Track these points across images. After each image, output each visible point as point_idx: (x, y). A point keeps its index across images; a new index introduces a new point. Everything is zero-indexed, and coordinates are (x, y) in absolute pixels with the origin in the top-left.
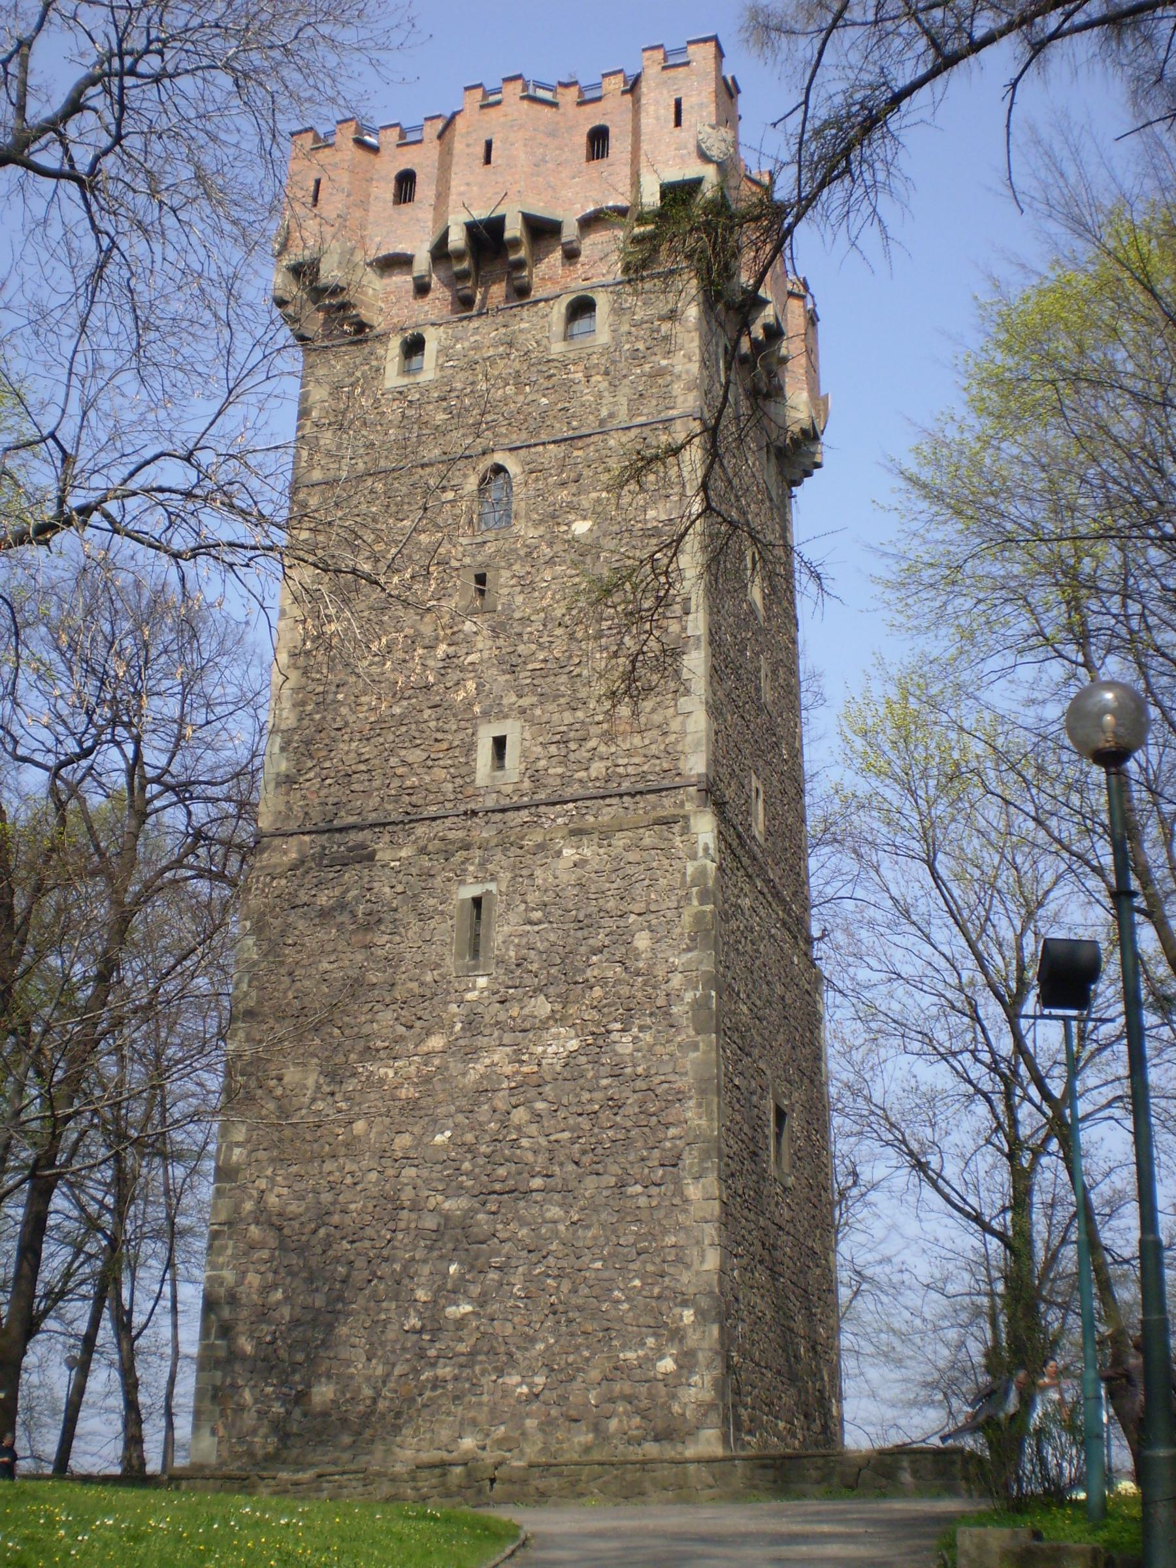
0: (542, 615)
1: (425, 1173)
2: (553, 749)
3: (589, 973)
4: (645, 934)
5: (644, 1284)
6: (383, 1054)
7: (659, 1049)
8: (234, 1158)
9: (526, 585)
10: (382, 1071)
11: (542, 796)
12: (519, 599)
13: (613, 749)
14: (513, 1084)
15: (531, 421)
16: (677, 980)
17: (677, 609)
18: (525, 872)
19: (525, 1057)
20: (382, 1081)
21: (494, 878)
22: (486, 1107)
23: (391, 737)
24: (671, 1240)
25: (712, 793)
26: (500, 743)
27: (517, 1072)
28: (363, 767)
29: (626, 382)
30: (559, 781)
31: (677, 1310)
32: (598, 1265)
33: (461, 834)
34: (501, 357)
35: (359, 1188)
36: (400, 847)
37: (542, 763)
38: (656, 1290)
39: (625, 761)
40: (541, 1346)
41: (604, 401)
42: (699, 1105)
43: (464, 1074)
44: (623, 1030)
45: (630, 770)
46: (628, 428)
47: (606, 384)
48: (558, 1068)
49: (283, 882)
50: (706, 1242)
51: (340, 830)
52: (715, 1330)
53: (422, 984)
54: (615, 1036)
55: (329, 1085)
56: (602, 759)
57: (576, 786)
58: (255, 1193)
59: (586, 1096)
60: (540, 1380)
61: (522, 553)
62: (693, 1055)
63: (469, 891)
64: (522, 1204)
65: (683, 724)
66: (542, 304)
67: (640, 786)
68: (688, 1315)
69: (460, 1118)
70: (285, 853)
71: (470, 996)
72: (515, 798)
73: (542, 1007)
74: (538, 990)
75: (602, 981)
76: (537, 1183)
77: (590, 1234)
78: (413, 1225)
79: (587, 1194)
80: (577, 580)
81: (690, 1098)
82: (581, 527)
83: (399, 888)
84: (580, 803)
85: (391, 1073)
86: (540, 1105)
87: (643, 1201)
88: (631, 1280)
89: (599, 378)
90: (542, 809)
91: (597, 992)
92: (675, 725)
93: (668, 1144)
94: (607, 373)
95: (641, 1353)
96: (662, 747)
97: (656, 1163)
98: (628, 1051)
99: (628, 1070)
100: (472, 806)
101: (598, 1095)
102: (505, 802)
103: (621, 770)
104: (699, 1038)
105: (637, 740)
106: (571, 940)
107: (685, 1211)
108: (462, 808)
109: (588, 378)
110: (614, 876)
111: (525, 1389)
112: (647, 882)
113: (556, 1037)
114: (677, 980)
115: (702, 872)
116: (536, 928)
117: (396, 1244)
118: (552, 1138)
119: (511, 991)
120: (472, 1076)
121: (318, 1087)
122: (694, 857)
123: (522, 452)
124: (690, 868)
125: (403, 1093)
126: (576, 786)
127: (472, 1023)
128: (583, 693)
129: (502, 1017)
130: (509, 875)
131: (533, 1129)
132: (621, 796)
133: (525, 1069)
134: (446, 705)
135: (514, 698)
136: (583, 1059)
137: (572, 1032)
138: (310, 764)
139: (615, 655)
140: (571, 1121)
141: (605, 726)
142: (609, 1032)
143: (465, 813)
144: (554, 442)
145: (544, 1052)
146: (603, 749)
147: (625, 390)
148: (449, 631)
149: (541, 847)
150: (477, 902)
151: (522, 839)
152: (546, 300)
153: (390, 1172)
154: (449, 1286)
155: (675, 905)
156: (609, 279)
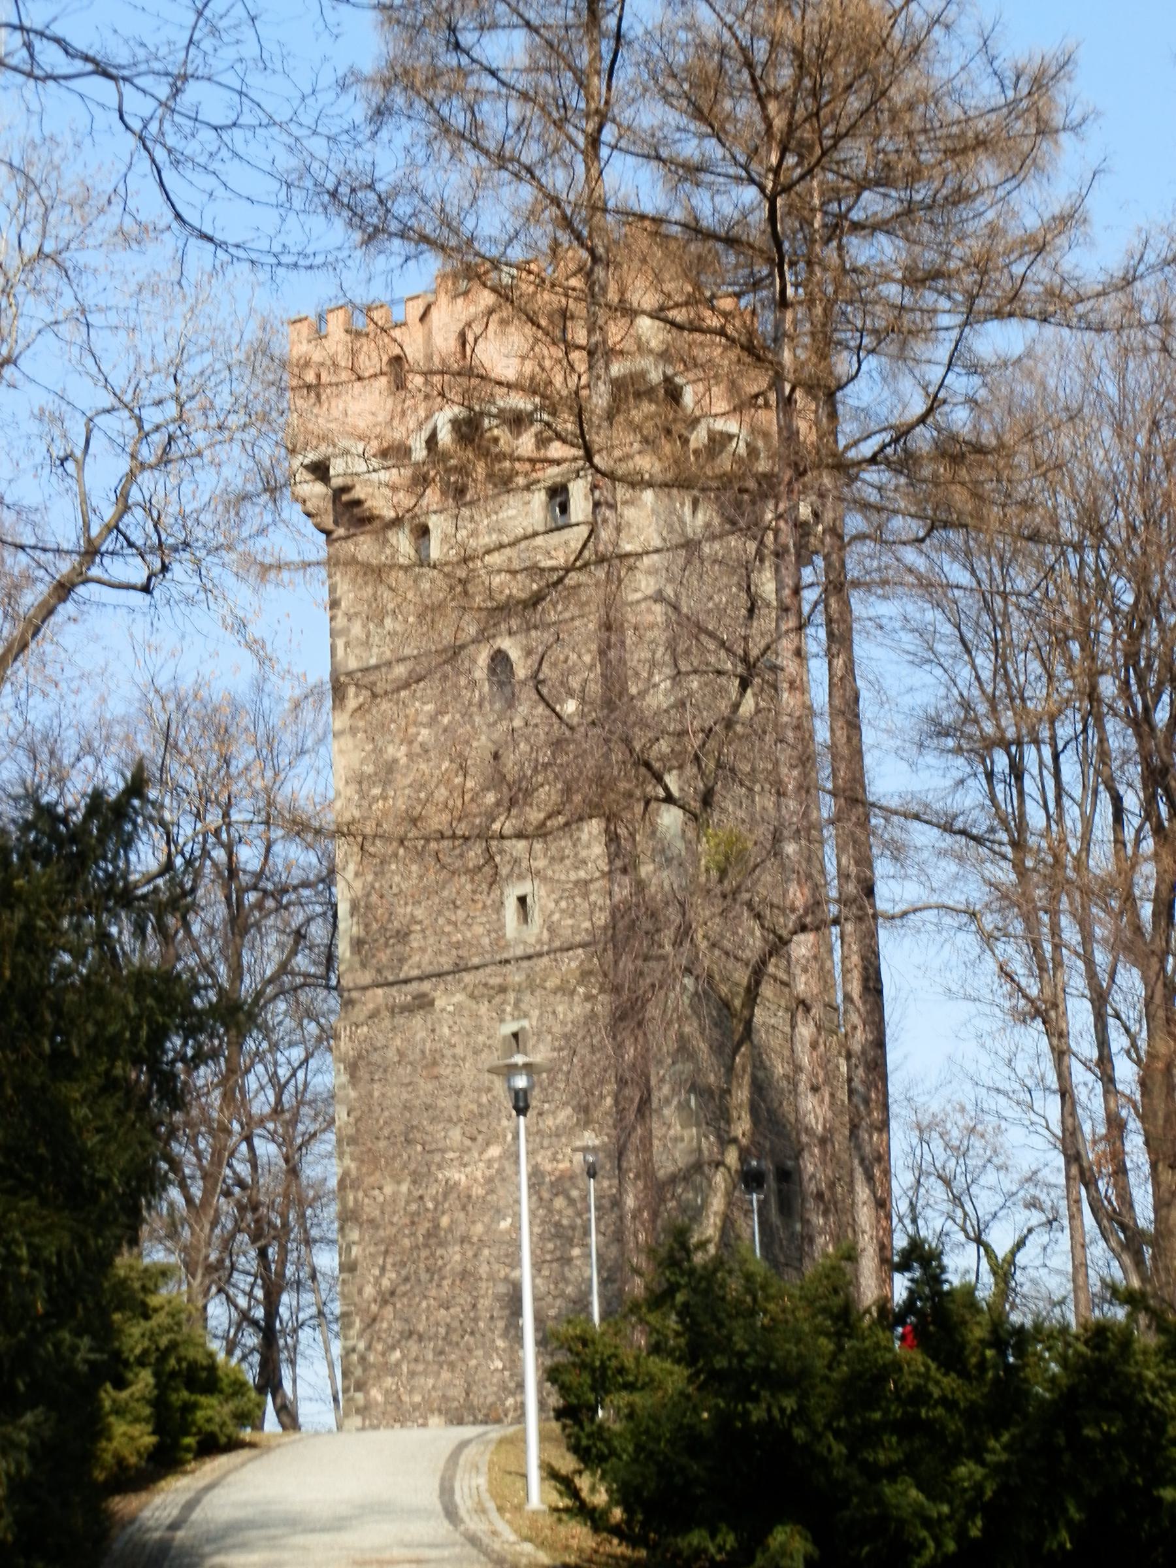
11: (557, 944)
21: (526, 1016)
26: (522, 900)
51: (406, 981)
63: (509, 1028)
100: (505, 956)
102: (530, 951)
128: (584, 853)
150: (515, 1035)
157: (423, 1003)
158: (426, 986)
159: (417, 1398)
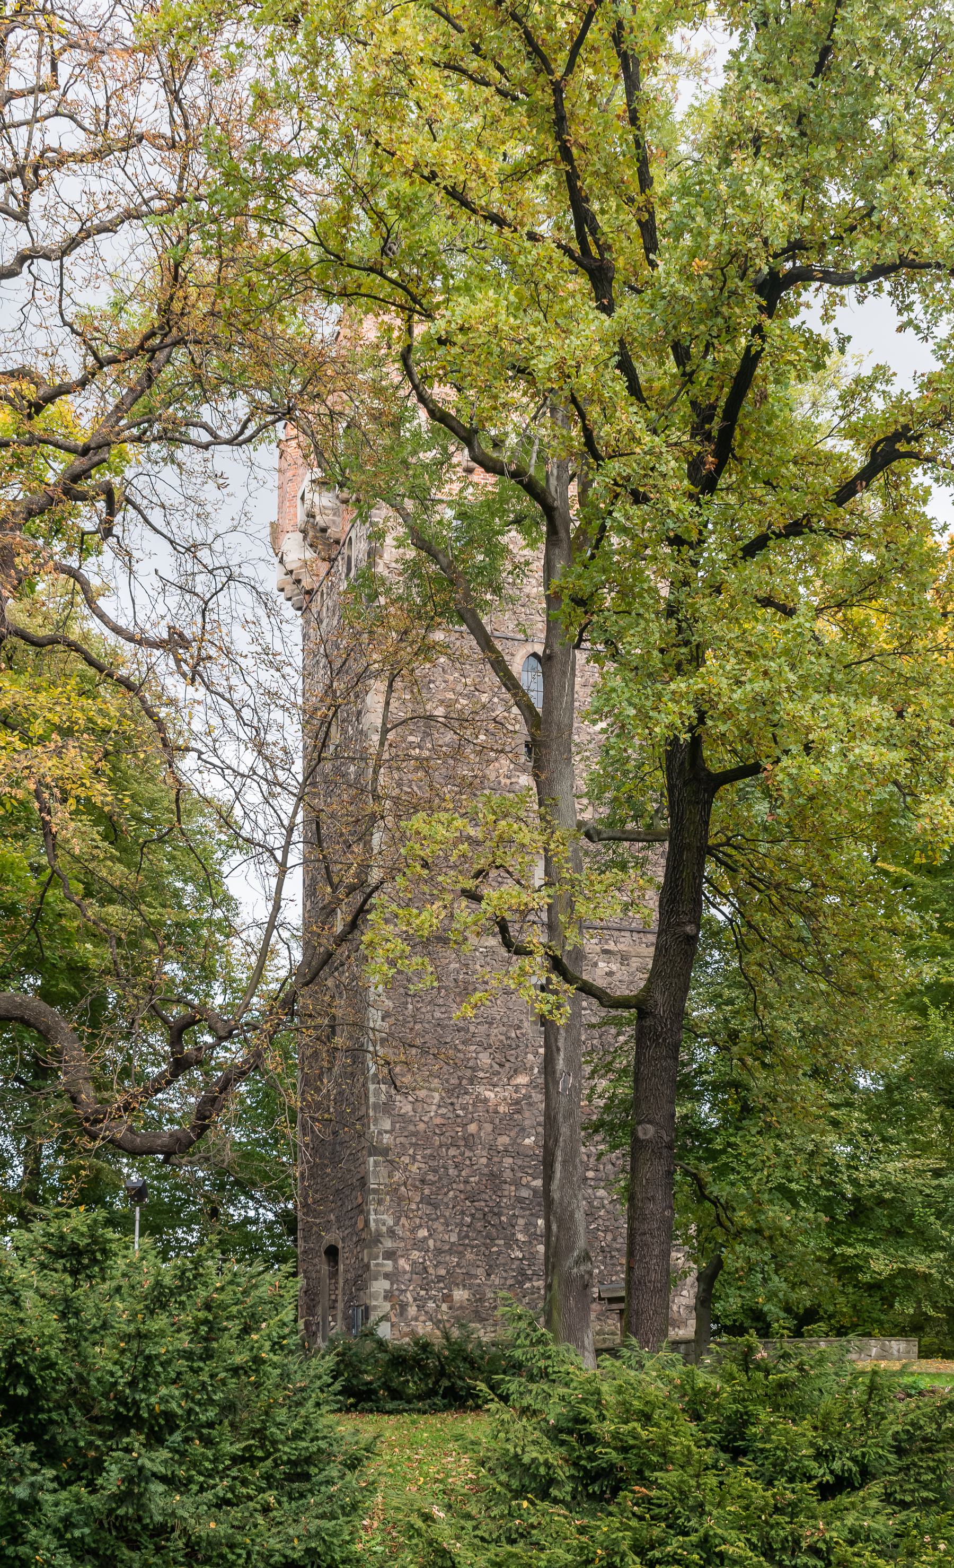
1: (520, 1163)
53: (508, 1038)
153: (496, 1159)
159: (443, 1272)
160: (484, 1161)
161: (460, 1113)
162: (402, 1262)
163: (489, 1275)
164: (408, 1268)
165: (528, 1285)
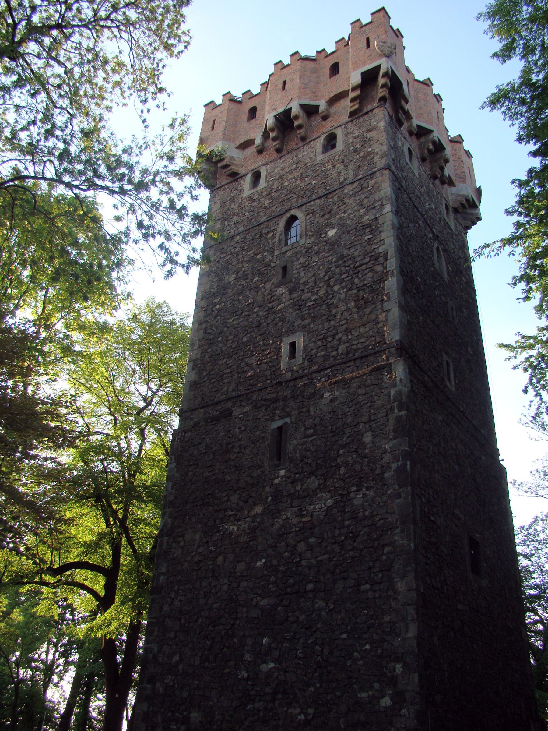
0: (314, 278)
2: (319, 343)
3: (339, 460)
4: (369, 434)
5: (371, 647)
6: (232, 518)
7: (378, 499)
8: (161, 581)
9: (305, 267)
10: (231, 527)
12: (302, 274)
13: (350, 337)
14: (297, 529)
15: (308, 192)
16: (387, 458)
17: (381, 259)
18: (304, 410)
19: (304, 513)
20: (231, 533)
21: (289, 415)
22: (283, 543)
23: (242, 354)
24: (387, 618)
25: (402, 349)
26: (293, 345)
27: (300, 522)
28: (228, 371)
29: (352, 163)
30: (322, 359)
31: (391, 665)
32: (345, 636)
33: (274, 396)
34: (295, 169)
35: (219, 594)
36: (244, 406)
37: (314, 351)
38: (379, 651)
39: (356, 342)
40: (312, 689)
41: (342, 174)
42: (402, 531)
43: (273, 525)
44: (357, 491)
45: (359, 346)
46: (354, 182)
47: (343, 167)
48: (322, 517)
49: (190, 434)
50: (409, 618)
51: (217, 404)
52: (416, 677)
54: (352, 495)
55: (206, 538)
56: (344, 343)
57: (332, 360)
58: (169, 599)
59: (337, 532)
60: (311, 711)
61: (304, 252)
62: (398, 501)
64: (302, 600)
65: (386, 316)
66: (312, 142)
67: (365, 354)
68: (399, 668)
69: (270, 551)
70: (192, 419)
71: (276, 481)
72: (301, 372)
73: (313, 482)
74: (312, 473)
75: (346, 464)
76: (310, 586)
77: (340, 617)
78: (245, 615)
79: (338, 592)
80: (330, 258)
81: (397, 527)
82: (332, 233)
83: (243, 428)
84: (333, 368)
85: (236, 529)
86: (312, 540)
87: (370, 595)
88: (364, 645)
89: (339, 165)
90: (314, 375)
91: (343, 470)
92: (382, 317)
93: (384, 557)
94: (343, 162)
95: (370, 693)
96: (376, 330)
97: (378, 570)
98: (360, 503)
99: (361, 514)
101: (344, 531)
102: (295, 375)
103: (354, 347)
104: (401, 490)
105: (362, 330)
106: (328, 443)
107: (395, 599)
108: (274, 382)
109: (334, 167)
110: (351, 404)
111: (302, 717)
112: (368, 405)
113: (320, 499)
114: (387, 458)
115: (399, 393)
116: (310, 439)
117: (236, 626)
118: (318, 559)
119: (297, 476)
120: (276, 526)
121: (201, 539)
122: (395, 386)
123: (304, 207)
124: (393, 392)
125: (241, 539)
126: (332, 360)
127: (277, 496)
129: (292, 491)
130: (297, 413)
131: (308, 554)
132: (355, 360)
133: (304, 519)
134: (267, 332)
135: (300, 322)
136: (335, 510)
137: (329, 496)
138: (205, 373)
139: (350, 289)
140: (329, 548)
141: (345, 326)
142: (349, 493)
143: (276, 383)
144: (318, 198)
145: (314, 508)
146: (344, 338)
147: (351, 167)
148: (269, 297)
149: (313, 395)
150: (280, 428)
151: (304, 392)
152: (314, 140)
153: (235, 585)
154: (262, 652)
155: (384, 414)
156: (344, 122)
157: (227, 414)
158: (229, 405)
159: (185, 694)
160: (225, 587)
161: (212, 548)
162: (158, 685)
163: (220, 697)
164: (161, 690)
165: (250, 707)
